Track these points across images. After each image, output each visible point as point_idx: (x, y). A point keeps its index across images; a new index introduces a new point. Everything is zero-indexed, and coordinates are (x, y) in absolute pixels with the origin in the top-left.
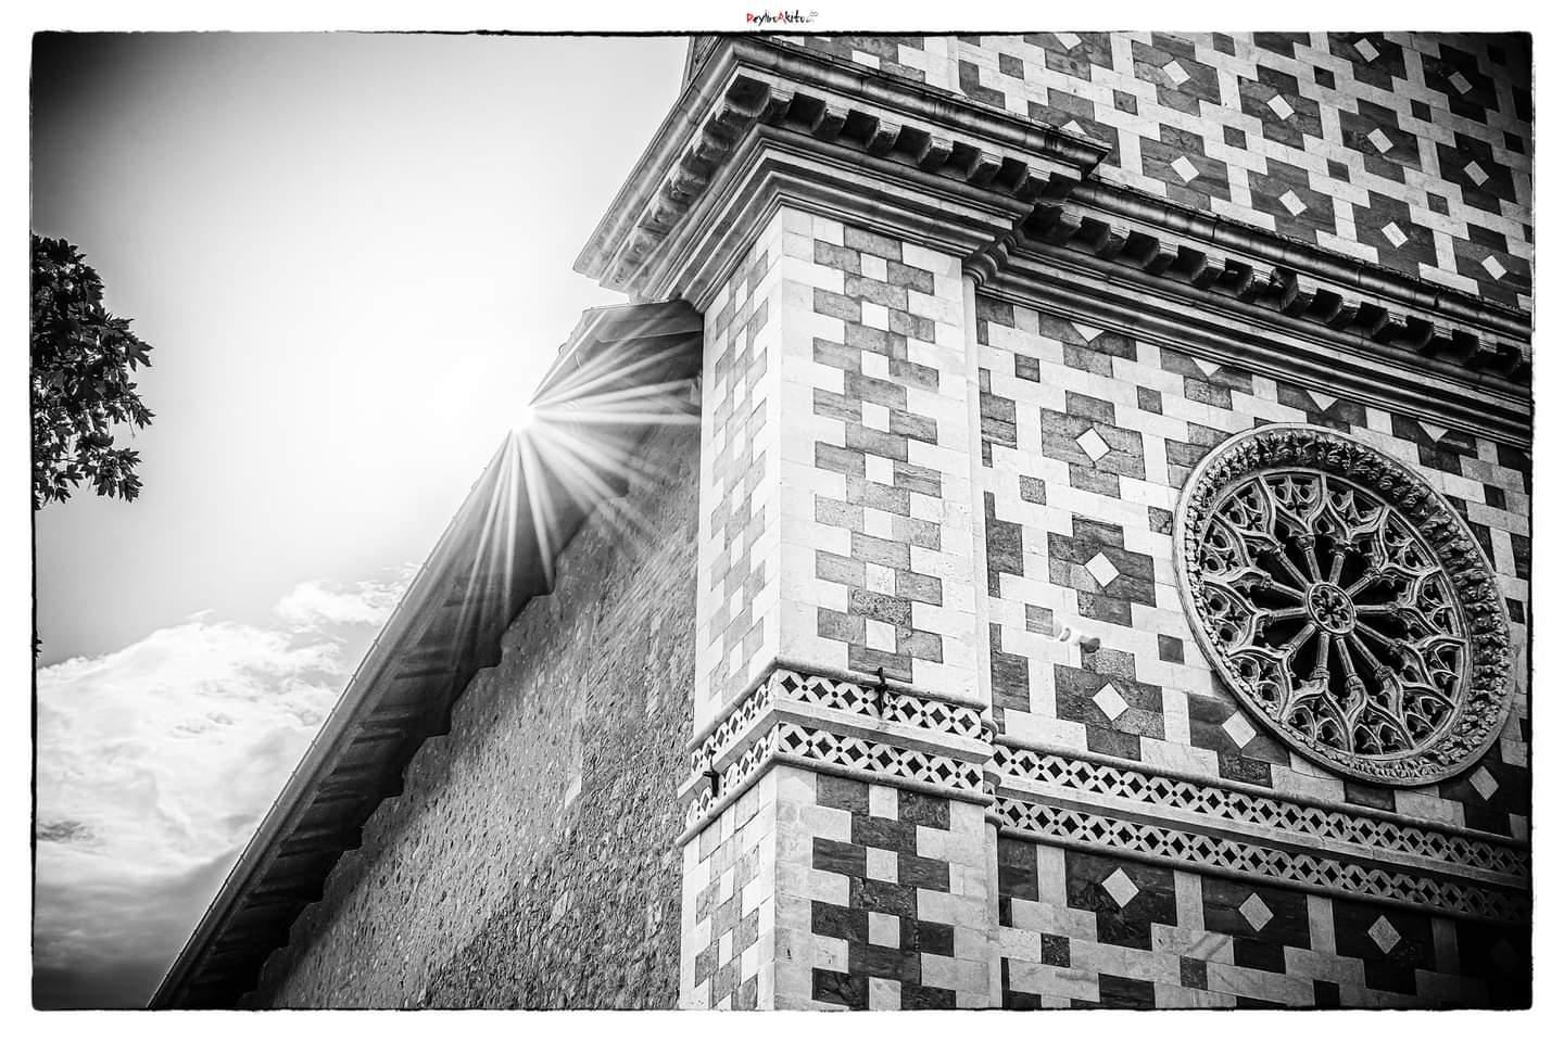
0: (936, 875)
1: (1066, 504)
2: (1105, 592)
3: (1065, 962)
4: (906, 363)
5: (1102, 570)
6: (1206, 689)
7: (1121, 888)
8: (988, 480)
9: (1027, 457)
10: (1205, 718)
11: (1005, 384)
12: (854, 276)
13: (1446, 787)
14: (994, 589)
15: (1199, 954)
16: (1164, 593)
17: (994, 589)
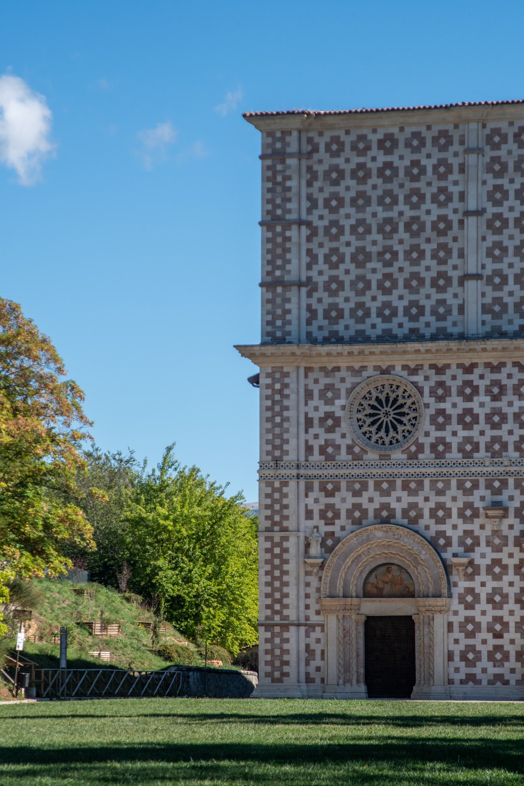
0: (286, 496)
1: (324, 409)
2: (330, 427)
3: (318, 502)
4: (283, 395)
5: (330, 422)
6: (350, 442)
7: (330, 487)
8: (307, 409)
9: (316, 401)
10: (350, 449)
11: (311, 386)
12: (273, 379)
13: (403, 452)
14: (307, 432)
15: (345, 496)
16: (343, 424)
17: (307, 432)
